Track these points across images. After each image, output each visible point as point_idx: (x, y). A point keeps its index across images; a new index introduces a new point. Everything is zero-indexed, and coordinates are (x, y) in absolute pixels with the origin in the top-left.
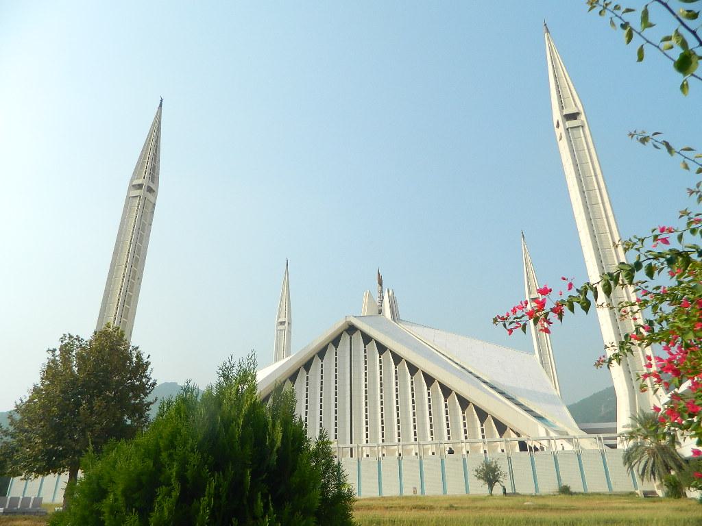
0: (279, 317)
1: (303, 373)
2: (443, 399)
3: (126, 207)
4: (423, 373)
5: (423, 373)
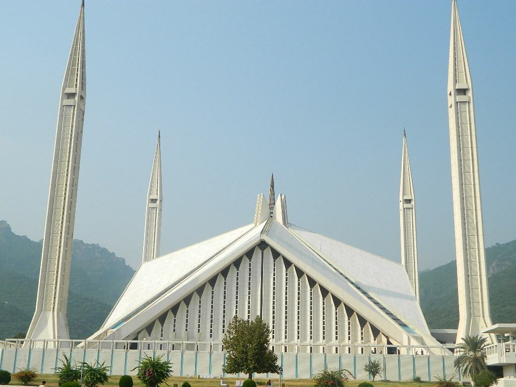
0: (150, 194)
1: (221, 279)
2: (334, 308)
3: (61, 115)
4: (320, 286)
5: (320, 286)
